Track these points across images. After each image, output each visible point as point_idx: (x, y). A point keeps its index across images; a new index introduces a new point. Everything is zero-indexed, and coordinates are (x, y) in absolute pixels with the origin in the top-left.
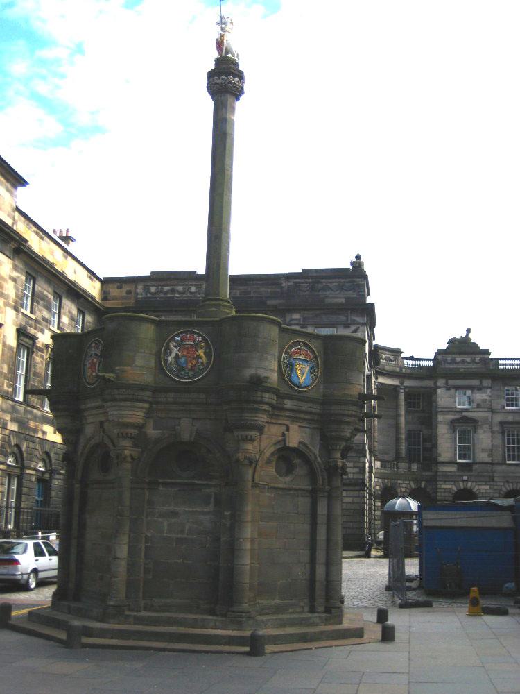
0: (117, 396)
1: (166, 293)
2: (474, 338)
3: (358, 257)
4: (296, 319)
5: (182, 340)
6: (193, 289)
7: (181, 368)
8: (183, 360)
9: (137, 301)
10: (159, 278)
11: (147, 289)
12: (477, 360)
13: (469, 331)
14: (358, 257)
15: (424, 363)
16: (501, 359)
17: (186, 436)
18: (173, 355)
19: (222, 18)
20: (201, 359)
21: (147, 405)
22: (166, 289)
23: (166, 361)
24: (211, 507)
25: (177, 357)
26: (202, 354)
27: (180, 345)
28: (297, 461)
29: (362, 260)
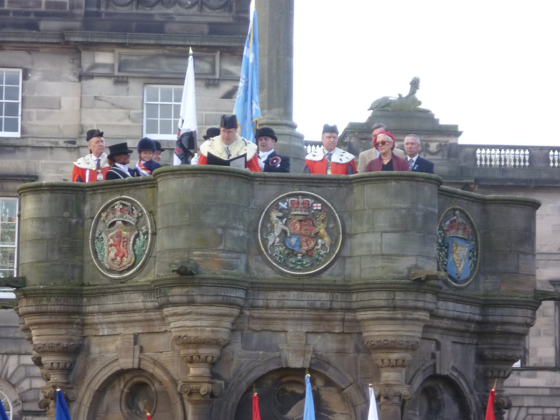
0: (198, 299)
2: (427, 100)
4: (104, 65)
5: (289, 209)
7: (292, 253)
8: (293, 240)
12: (433, 147)
13: (415, 84)
16: (481, 147)
18: (277, 232)
20: (322, 238)
21: (236, 311)
23: (265, 241)
26: (322, 231)
27: (285, 215)
28: (446, 396)
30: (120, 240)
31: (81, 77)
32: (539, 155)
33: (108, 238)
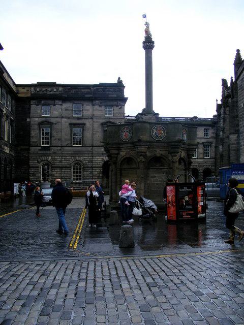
1: (44, 91)
3: (119, 78)
6: (55, 90)
9: (32, 94)
10: (40, 85)
11: (35, 89)
14: (119, 78)
15: (132, 118)
17: (158, 155)
19: (146, 23)
22: (44, 89)
24: (165, 174)
25: (156, 133)
27: (156, 130)
29: (121, 79)
30: (126, 135)
31: (93, 105)
32: (173, 118)
33: (123, 134)
